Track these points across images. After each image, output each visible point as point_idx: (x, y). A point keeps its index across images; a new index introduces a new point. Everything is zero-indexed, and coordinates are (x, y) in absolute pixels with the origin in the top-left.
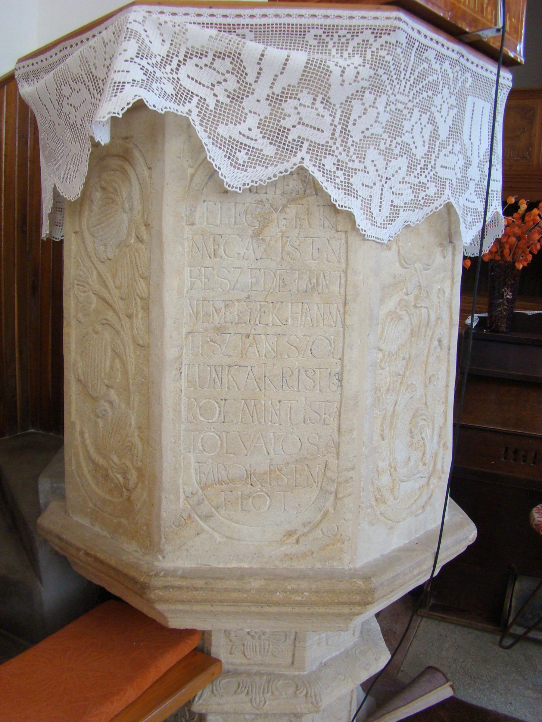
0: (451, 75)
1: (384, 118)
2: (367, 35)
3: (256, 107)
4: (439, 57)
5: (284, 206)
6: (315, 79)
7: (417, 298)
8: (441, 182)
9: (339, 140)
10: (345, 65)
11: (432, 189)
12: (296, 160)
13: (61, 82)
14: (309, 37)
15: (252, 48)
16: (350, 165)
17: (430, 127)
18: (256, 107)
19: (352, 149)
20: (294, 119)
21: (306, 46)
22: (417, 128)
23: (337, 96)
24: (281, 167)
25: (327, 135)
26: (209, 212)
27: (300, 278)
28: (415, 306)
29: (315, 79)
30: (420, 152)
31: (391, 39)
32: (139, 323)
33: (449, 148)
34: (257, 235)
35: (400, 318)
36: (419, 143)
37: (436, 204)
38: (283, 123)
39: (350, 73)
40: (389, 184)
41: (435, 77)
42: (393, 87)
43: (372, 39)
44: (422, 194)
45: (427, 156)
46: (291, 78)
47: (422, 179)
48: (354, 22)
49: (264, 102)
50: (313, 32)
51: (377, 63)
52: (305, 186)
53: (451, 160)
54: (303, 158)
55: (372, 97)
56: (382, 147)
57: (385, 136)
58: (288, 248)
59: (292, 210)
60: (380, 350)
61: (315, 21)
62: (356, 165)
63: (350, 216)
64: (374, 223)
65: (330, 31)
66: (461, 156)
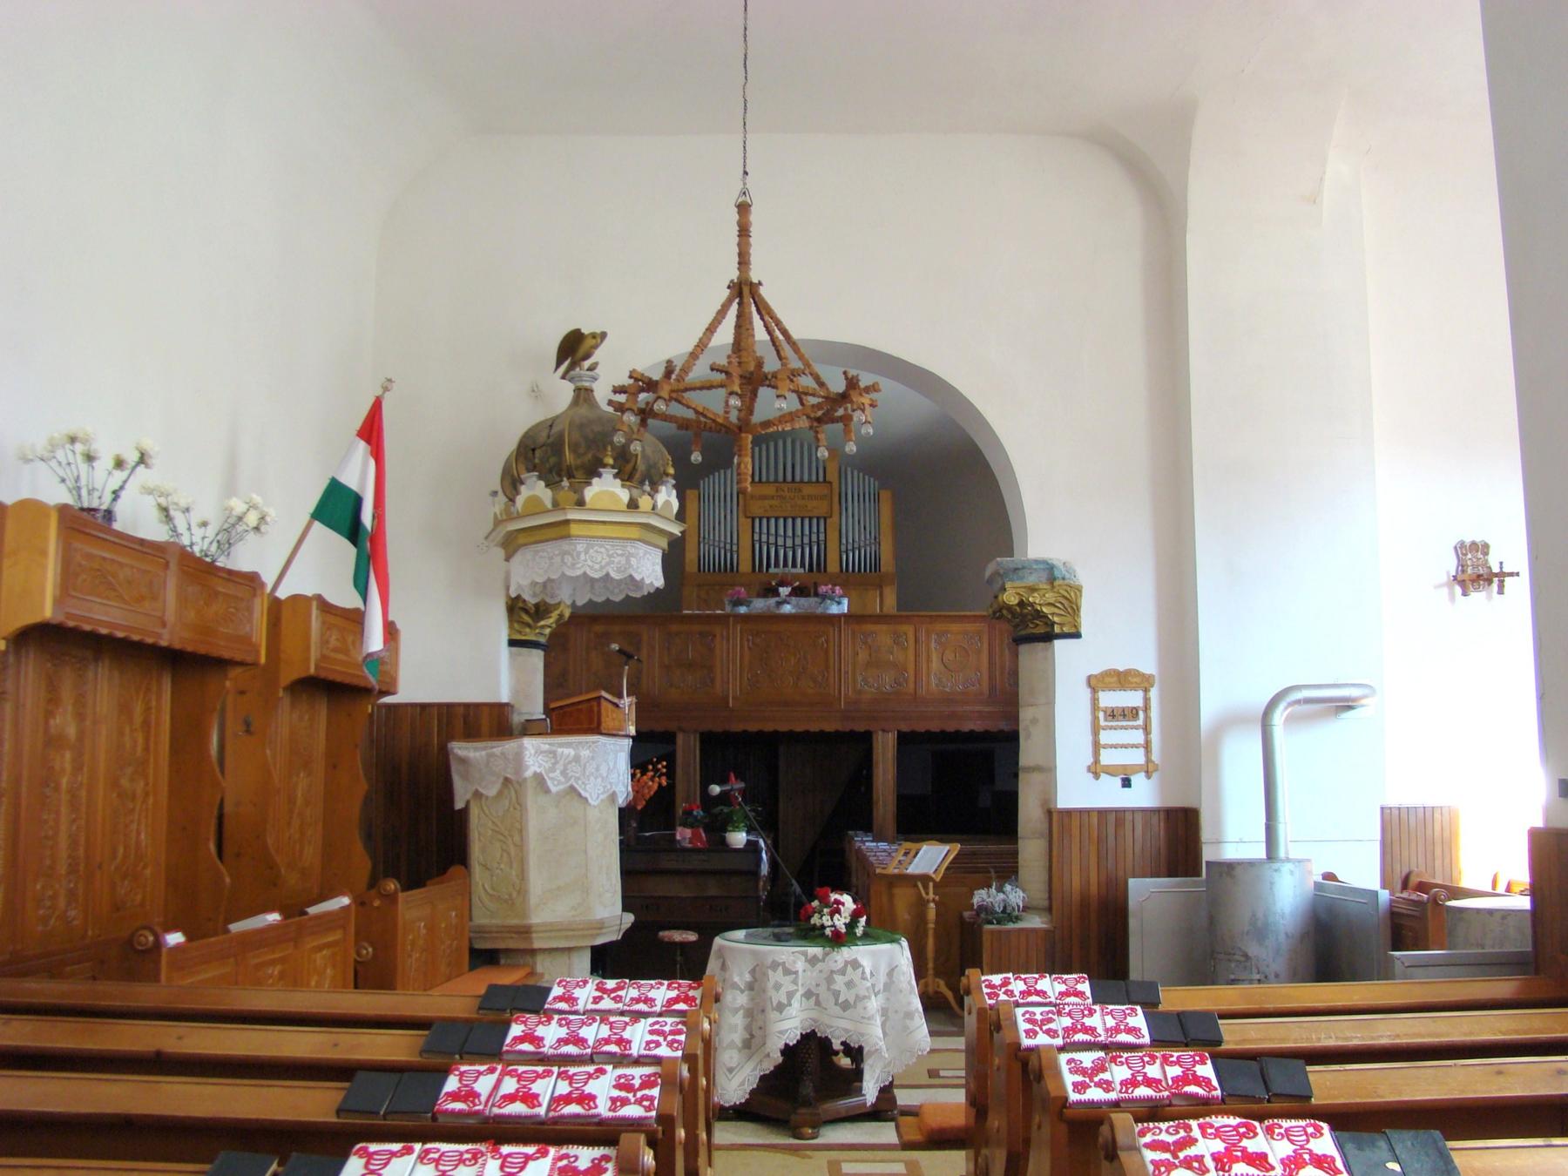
3: (560, 767)
6: (577, 759)
10: (585, 753)
13: (490, 756)
15: (560, 750)
18: (560, 767)
29: (577, 759)
32: (517, 838)
52: (572, 788)
54: (572, 782)
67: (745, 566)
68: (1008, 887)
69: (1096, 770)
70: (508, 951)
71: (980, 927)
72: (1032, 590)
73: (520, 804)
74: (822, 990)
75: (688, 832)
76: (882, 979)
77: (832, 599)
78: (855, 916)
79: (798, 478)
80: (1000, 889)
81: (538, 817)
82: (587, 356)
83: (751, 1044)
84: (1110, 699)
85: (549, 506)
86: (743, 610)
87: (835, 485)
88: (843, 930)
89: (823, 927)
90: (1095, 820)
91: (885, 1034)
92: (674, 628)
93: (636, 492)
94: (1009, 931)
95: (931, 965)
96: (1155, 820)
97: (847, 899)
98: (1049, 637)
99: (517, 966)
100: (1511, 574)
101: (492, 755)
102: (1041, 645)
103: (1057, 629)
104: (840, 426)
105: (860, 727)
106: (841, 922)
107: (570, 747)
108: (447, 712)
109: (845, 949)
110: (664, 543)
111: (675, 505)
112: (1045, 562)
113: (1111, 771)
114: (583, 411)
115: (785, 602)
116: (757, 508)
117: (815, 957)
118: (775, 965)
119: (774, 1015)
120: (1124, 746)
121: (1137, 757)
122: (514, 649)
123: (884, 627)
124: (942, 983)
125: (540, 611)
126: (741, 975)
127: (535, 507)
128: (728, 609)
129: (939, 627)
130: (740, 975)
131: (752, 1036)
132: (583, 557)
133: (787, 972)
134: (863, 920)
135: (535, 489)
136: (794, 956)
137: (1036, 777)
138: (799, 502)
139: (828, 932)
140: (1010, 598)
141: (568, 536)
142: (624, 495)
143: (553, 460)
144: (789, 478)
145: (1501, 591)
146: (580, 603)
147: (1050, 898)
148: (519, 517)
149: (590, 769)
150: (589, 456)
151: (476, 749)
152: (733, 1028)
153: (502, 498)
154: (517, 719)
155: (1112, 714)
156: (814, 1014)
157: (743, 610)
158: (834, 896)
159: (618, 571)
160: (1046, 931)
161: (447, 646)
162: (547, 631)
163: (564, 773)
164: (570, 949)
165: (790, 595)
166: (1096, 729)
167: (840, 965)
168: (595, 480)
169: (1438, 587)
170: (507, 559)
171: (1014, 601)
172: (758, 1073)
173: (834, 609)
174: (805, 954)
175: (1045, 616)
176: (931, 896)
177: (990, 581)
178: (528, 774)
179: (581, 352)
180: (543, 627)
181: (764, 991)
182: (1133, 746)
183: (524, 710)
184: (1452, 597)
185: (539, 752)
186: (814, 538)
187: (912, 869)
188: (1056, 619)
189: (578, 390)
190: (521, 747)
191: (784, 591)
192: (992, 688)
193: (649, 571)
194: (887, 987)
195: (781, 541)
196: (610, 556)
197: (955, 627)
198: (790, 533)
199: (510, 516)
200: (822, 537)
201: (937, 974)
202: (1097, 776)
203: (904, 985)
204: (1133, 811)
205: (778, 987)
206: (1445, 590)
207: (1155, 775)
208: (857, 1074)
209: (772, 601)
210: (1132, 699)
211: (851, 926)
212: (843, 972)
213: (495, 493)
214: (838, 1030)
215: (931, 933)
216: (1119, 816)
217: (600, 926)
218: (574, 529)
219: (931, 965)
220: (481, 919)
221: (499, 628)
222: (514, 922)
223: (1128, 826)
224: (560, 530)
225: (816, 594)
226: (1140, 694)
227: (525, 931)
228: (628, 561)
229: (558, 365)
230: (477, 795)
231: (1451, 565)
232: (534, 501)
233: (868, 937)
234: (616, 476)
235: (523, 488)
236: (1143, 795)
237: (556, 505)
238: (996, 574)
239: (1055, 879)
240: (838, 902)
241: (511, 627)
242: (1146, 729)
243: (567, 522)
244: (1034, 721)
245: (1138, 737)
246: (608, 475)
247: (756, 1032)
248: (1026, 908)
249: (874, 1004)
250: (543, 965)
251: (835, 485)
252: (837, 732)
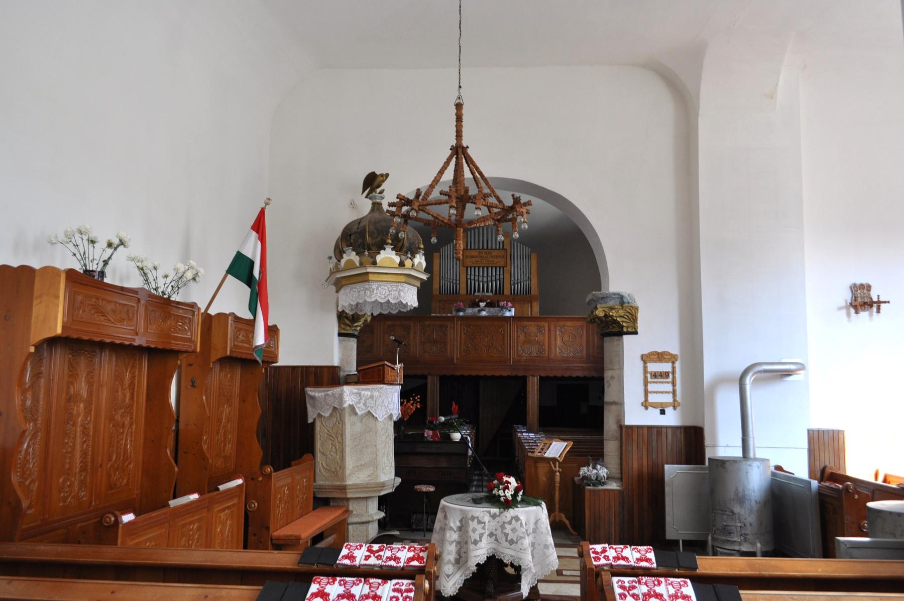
3: (363, 401)
6: (372, 397)
10: (376, 394)
18: (363, 401)
26: (353, 418)
29: (372, 397)
32: (340, 439)
52: (369, 412)
54: (369, 409)
68: (599, 467)
69: (646, 405)
70: (334, 499)
71: (584, 488)
72: (612, 308)
73: (342, 421)
74: (499, 533)
75: (431, 433)
76: (532, 526)
78: (517, 490)
80: (594, 468)
81: (351, 428)
82: (379, 186)
83: (460, 560)
84: (653, 367)
85: (358, 264)
88: (510, 498)
89: (499, 496)
90: (646, 431)
91: (533, 557)
93: (403, 257)
94: (599, 490)
95: (557, 506)
96: (678, 432)
97: (512, 480)
98: (621, 334)
99: (339, 507)
100: (885, 302)
101: (328, 395)
102: (616, 338)
103: (625, 330)
104: (510, 223)
106: (509, 494)
107: (367, 391)
108: (306, 369)
109: (511, 510)
110: (418, 284)
111: (424, 264)
112: (619, 294)
113: (654, 405)
114: (376, 215)
117: (495, 514)
118: (473, 518)
119: (472, 547)
120: (661, 392)
121: (669, 398)
124: (563, 515)
125: (355, 318)
126: (454, 522)
127: (350, 265)
130: (454, 523)
131: (460, 557)
133: (479, 522)
134: (521, 493)
135: (351, 256)
136: (483, 512)
137: (613, 407)
139: (502, 499)
140: (600, 313)
141: (368, 281)
142: (397, 259)
143: (360, 241)
145: (878, 311)
146: (375, 314)
147: (621, 473)
148: (344, 270)
149: (379, 402)
150: (379, 239)
151: (319, 392)
152: (450, 553)
153: (334, 260)
154: (342, 374)
155: (655, 375)
156: (494, 546)
158: (505, 479)
160: (619, 491)
161: (307, 337)
162: (359, 328)
163: (365, 404)
164: (367, 498)
166: (646, 383)
167: (508, 519)
168: (382, 252)
169: (840, 309)
170: (337, 292)
171: (602, 314)
172: (464, 578)
174: (489, 512)
175: (618, 322)
176: (557, 469)
177: (589, 303)
178: (346, 405)
179: (376, 183)
181: (467, 532)
182: (666, 392)
183: (346, 369)
184: (849, 315)
185: (352, 393)
187: (546, 455)
189: (374, 204)
190: (342, 391)
193: (410, 298)
194: (535, 531)
199: (337, 269)
201: (560, 511)
202: (646, 408)
203: (544, 530)
204: (667, 427)
205: (474, 530)
206: (844, 311)
207: (678, 408)
208: (517, 578)
210: (666, 367)
211: (514, 496)
212: (510, 523)
213: (330, 258)
214: (507, 555)
215: (557, 489)
216: (659, 429)
217: (383, 485)
218: (371, 277)
219: (557, 506)
220: (320, 482)
221: (334, 327)
222: (338, 483)
223: (664, 435)
224: (364, 278)
226: (670, 365)
227: (343, 488)
228: (399, 294)
229: (363, 191)
230: (319, 415)
231: (848, 296)
232: (350, 262)
233: (526, 502)
234: (392, 249)
235: (344, 255)
236: (671, 419)
237: (362, 264)
238: (592, 300)
239: (624, 463)
240: (508, 482)
241: (339, 326)
242: (674, 383)
243: (367, 273)
244: (613, 378)
245: (669, 388)
246: (389, 249)
247: (463, 555)
248: (608, 478)
249: (527, 541)
250: (352, 506)
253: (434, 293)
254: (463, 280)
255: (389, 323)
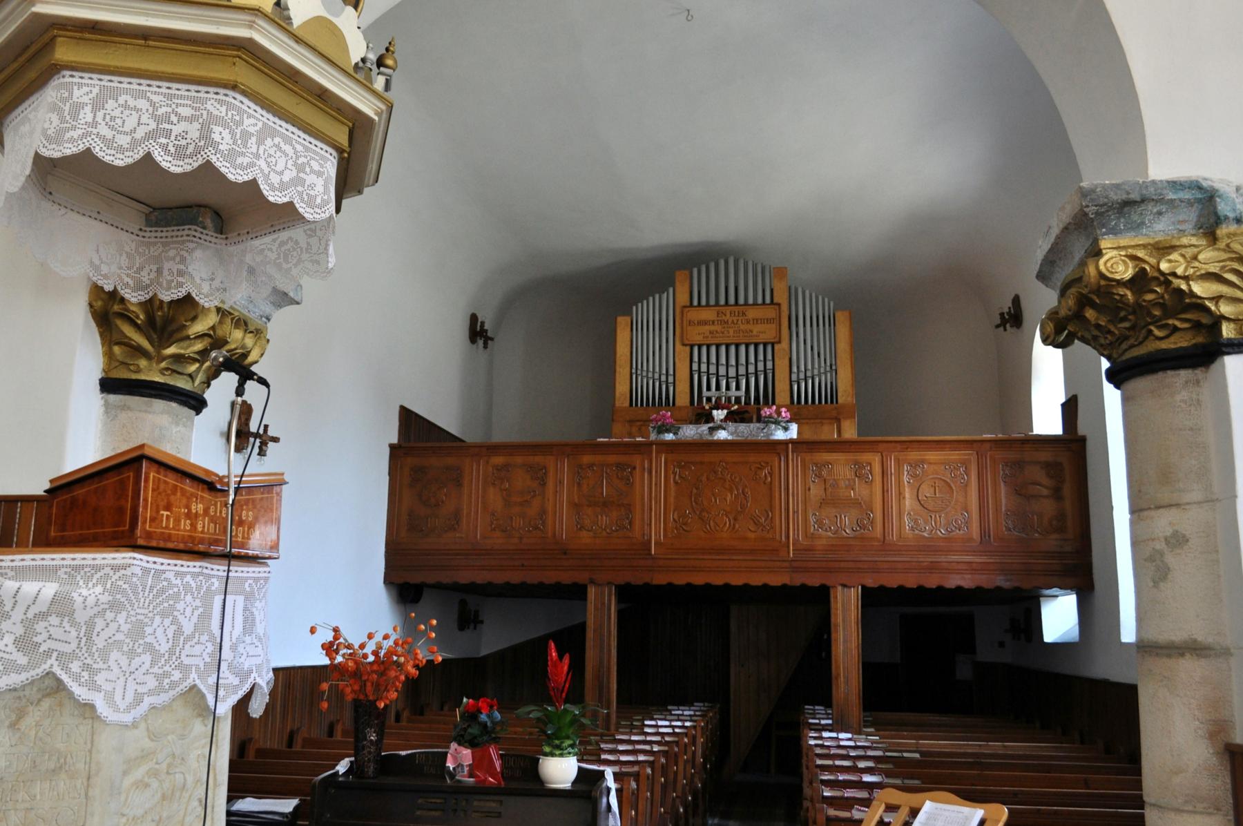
0: (194, 585)
1: (125, 628)
2: (108, 570)
4: (177, 574)
5: (40, 700)
7: (169, 766)
8: (185, 669)
9: (84, 649)
10: (88, 593)
11: (177, 675)
12: (46, 667)
14: (61, 573)
16: (95, 666)
17: (174, 627)
19: (96, 654)
20: (45, 635)
21: (58, 579)
22: (160, 631)
23: (81, 617)
24: (33, 673)
25: (74, 645)
27: (49, 759)
28: (168, 773)
29: (61, 607)
30: (164, 648)
31: (128, 572)
33: (195, 640)
34: (13, 726)
35: (147, 785)
36: (162, 639)
37: (181, 687)
38: (35, 639)
39: (91, 601)
40: (133, 676)
41: (176, 590)
42: (132, 605)
43: (111, 573)
44: (167, 681)
45: (171, 652)
46: (41, 606)
47: (167, 668)
48: (96, 562)
49: (19, 626)
50: (64, 570)
51: (115, 590)
53: (198, 649)
54: (52, 664)
55: (113, 615)
56: (125, 649)
57: (127, 641)
58: (41, 734)
59: (46, 704)
60: (123, 815)
61: (65, 563)
62: (101, 665)
63: (92, 707)
64: (117, 710)
65: (77, 568)
66: (209, 644)
67: (683, 400)
72: (1163, 249)
77: (777, 423)
79: (741, 301)
86: (669, 437)
87: (785, 308)
92: (587, 459)
102: (1184, 374)
103: (1227, 331)
105: (814, 581)
112: (1196, 186)
115: (720, 427)
116: (696, 335)
122: (113, 398)
123: (839, 457)
128: (653, 437)
129: (914, 455)
132: (87, 115)
138: (742, 327)
140: (1115, 263)
144: (732, 300)
157: (669, 437)
159: (180, 153)
163: (25, 643)
165: (727, 419)
171: (1125, 272)
173: (780, 435)
175: (1199, 306)
180: (178, 358)
186: (761, 366)
188: (1225, 309)
191: (719, 415)
192: (984, 532)
195: (722, 371)
196: (158, 120)
197: (932, 456)
198: (733, 362)
200: (769, 365)
209: (704, 428)
225: (759, 421)
228: (205, 133)
241: (109, 355)
251: (785, 308)
252: (784, 586)
253: (618, 404)
254: (683, 373)
255: (498, 460)
